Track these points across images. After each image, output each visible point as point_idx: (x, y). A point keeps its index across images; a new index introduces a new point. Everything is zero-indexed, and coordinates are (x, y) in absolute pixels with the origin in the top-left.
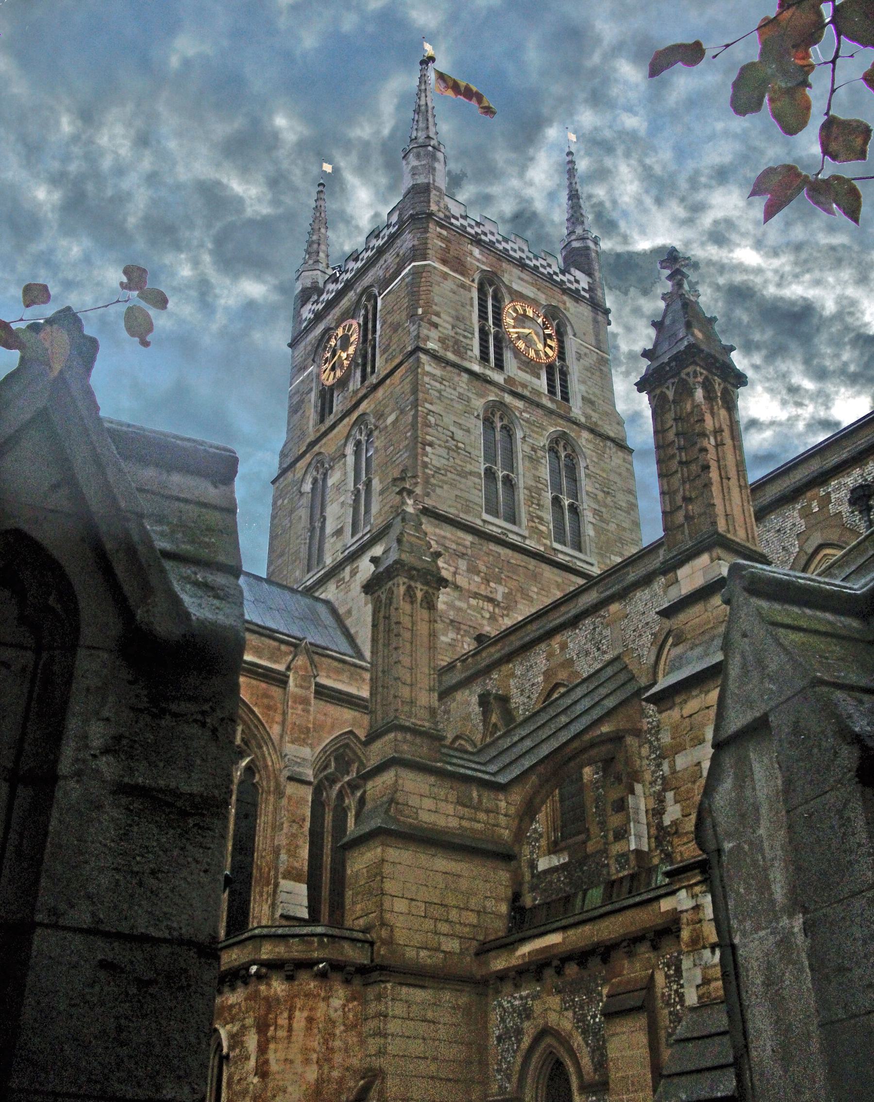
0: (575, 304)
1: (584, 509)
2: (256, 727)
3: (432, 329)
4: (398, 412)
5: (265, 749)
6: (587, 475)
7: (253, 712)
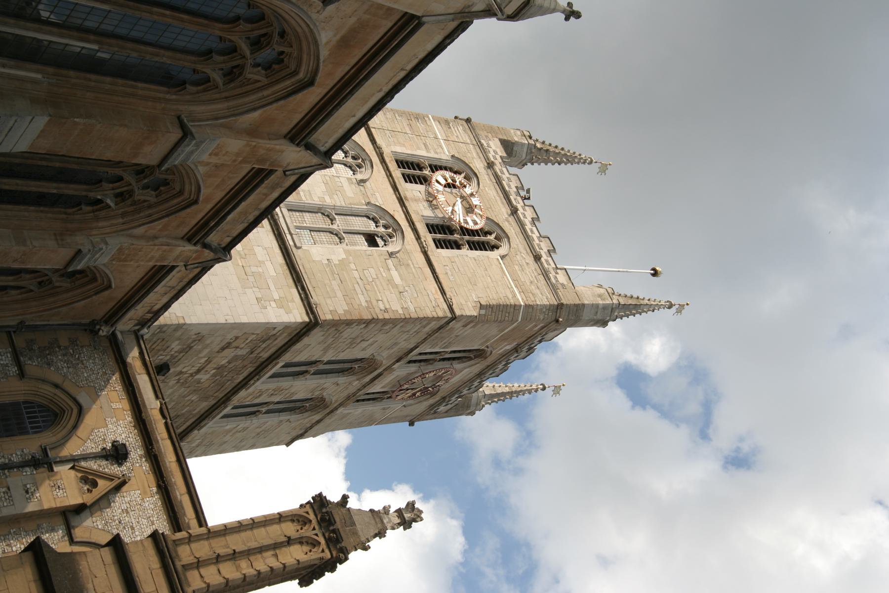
0: (429, 404)
1: (252, 420)
2: (150, 216)
3: (464, 324)
4: (401, 289)
5: (121, 220)
6: (281, 421)
7: (167, 216)
